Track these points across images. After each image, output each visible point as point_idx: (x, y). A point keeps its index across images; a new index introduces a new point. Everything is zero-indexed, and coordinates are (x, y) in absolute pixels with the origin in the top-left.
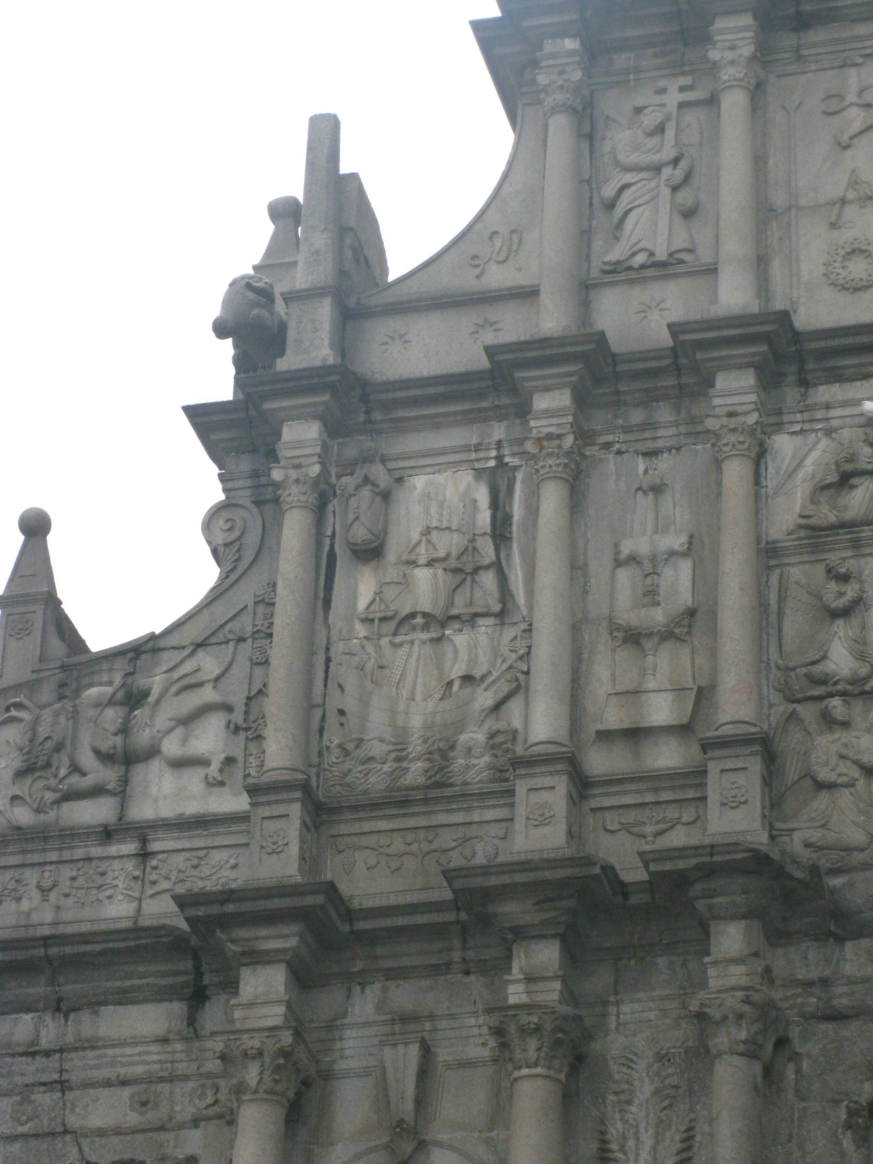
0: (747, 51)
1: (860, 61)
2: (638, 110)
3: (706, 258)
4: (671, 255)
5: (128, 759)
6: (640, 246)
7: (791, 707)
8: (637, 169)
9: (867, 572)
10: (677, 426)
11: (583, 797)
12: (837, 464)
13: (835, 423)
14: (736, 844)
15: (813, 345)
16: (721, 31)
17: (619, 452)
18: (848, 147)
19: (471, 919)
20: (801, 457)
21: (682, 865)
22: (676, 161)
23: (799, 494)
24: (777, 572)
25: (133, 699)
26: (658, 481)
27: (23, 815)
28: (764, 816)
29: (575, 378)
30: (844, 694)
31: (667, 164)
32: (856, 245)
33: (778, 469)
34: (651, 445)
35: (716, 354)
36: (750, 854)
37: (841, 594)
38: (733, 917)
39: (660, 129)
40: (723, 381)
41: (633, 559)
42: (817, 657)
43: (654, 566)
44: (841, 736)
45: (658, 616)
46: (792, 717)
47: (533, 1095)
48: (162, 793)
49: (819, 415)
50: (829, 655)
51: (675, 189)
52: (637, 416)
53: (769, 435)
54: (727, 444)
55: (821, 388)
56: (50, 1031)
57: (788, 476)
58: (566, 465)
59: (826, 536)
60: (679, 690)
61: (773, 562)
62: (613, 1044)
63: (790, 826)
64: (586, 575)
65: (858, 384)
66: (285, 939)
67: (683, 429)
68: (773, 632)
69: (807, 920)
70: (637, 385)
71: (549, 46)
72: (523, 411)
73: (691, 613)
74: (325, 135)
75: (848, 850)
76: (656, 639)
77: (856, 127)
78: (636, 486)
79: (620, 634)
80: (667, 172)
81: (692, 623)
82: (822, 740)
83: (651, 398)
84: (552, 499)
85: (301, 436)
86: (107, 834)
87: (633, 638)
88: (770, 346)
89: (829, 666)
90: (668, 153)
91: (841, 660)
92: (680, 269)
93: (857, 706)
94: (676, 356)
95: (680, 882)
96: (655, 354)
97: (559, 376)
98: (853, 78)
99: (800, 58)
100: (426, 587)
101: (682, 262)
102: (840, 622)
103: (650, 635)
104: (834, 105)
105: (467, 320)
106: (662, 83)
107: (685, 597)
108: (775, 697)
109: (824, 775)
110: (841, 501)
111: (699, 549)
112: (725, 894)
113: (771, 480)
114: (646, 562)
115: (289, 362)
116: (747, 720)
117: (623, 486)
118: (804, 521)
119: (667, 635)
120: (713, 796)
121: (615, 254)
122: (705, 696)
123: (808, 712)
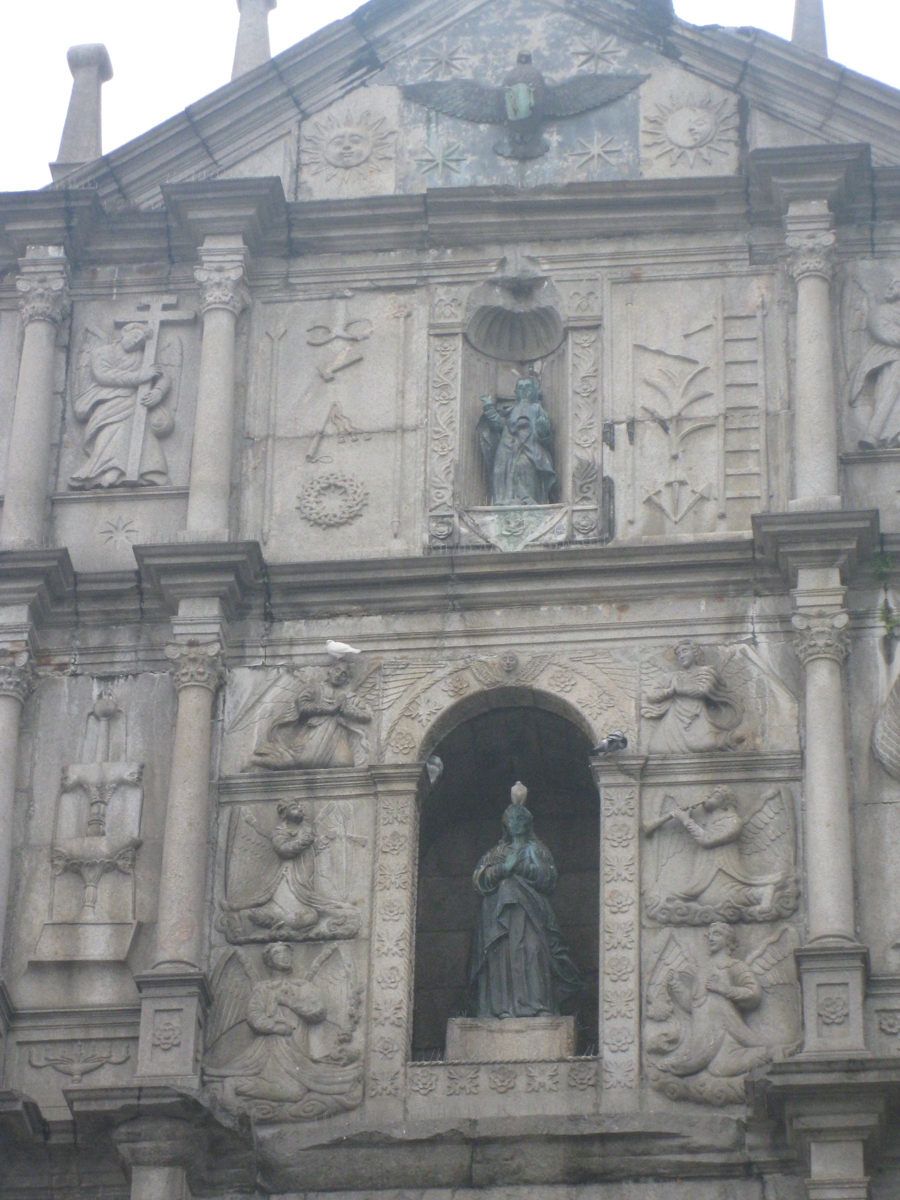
0: (235, 274)
1: (349, 294)
2: (119, 326)
3: (178, 481)
4: (142, 476)
6: (110, 464)
7: (232, 949)
8: (114, 385)
9: (320, 815)
10: (136, 652)
11: (9, 1030)
12: (297, 702)
13: (298, 660)
14: (166, 1088)
15: (281, 579)
16: (210, 252)
17: (74, 675)
18: (331, 379)
20: (260, 693)
21: (108, 1106)
22: (154, 381)
23: (256, 731)
24: (227, 811)
26: (111, 707)
28: (196, 1060)
29: (34, 595)
30: (287, 939)
31: (144, 383)
32: (332, 481)
33: (238, 702)
34: (108, 669)
35: (180, 581)
36: (179, 1099)
37: (292, 836)
38: (157, 1164)
39: (140, 347)
40: (185, 609)
41: (80, 786)
42: (263, 899)
43: (102, 795)
44: (281, 983)
45: (102, 846)
46: (233, 959)
49: (282, 651)
50: (275, 898)
51: (151, 409)
52: (95, 639)
53: (230, 668)
54: (186, 674)
55: (286, 623)
57: (247, 712)
58: (18, 684)
59: (280, 776)
60: (118, 924)
61: (224, 799)
63: (223, 1072)
64: (30, 801)
65: (325, 622)
67: (141, 655)
68: (220, 871)
69: (233, 1171)
70: (97, 607)
71: (32, 253)
73: (137, 846)
75: (281, 1100)
76: (98, 870)
77: (341, 360)
78: (90, 710)
79: (60, 863)
80: (144, 390)
81: (137, 856)
82: (262, 986)
83: (111, 621)
87: (74, 868)
88: (237, 577)
89: (275, 910)
90: (147, 371)
91: (286, 905)
92: (149, 491)
93: (301, 951)
94: (140, 580)
95: (104, 1124)
96: (118, 576)
97: (16, 591)
99: (288, 286)
101: (153, 484)
102: (289, 865)
103: (92, 865)
104: (320, 336)
106: (145, 300)
107: (131, 829)
108: (216, 938)
109: (261, 1021)
110: (298, 741)
111: (150, 780)
112: (151, 1140)
113: (228, 714)
114: (94, 790)
116: (185, 959)
117: (75, 710)
118: (258, 759)
119: (110, 867)
120: (146, 1035)
121: (85, 470)
122: (144, 931)
123: (249, 956)
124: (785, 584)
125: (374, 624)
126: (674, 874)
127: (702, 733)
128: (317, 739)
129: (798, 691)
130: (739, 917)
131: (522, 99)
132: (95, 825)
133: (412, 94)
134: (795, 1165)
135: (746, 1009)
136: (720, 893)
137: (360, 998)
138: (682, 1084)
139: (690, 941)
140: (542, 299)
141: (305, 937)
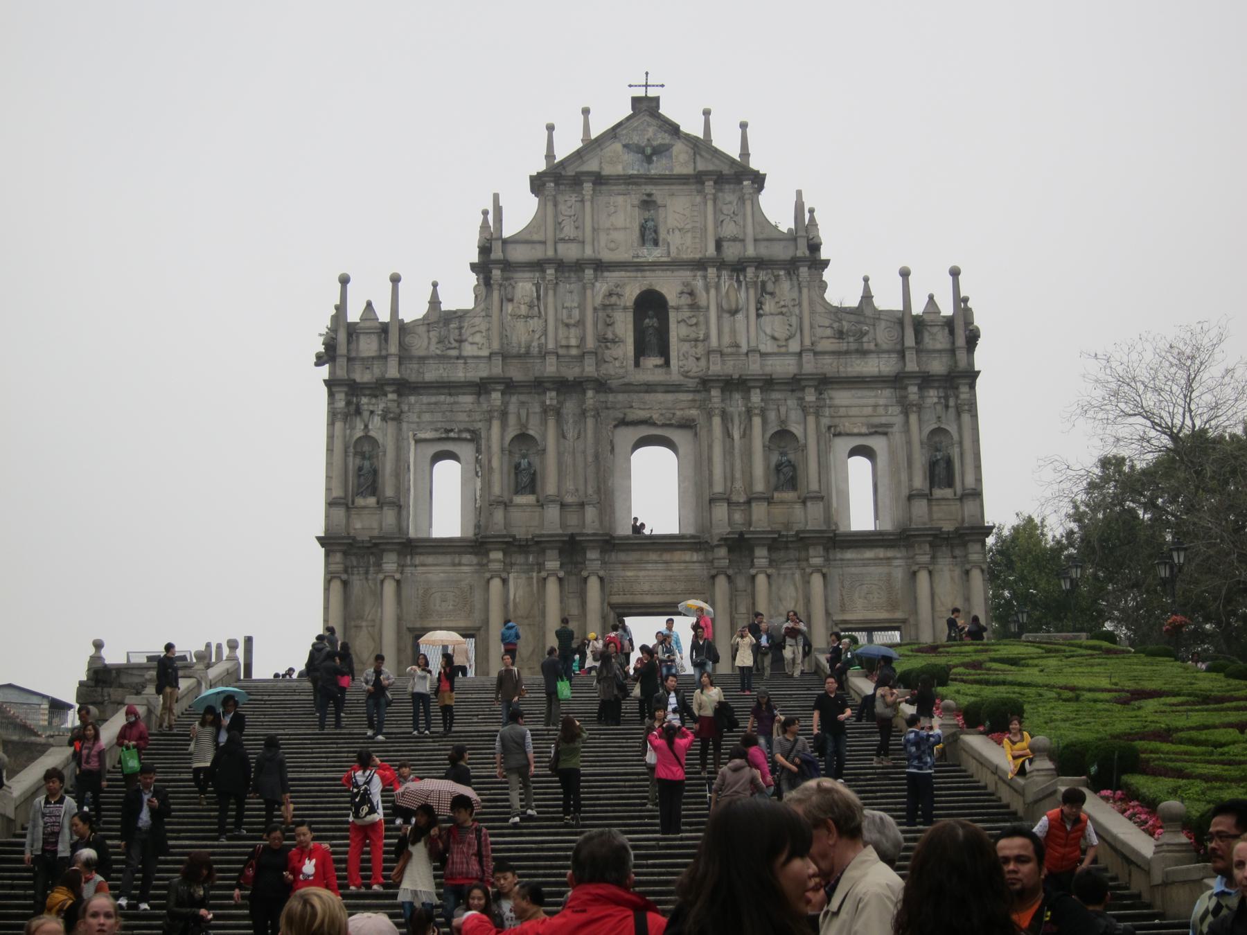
5: (460, 341)
19: (538, 385)
25: (460, 328)
27: (439, 352)
45: (572, 321)
47: (551, 423)
48: (468, 350)
56: (449, 399)
62: (564, 411)
66: (501, 387)
72: (543, 271)
74: (496, 197)
83: (570, 271)
84: (551, 293)
85: (496, 273)
86: (458, 358)
87: (567, 325)
91: (610, 336)
98: (612, 199)
100: (524, 310)
105: (529, 246)
107: (577, 318)
111: (582, 307)
115: (493, 256)
121: (562, 236)
122: (583, 339)
124: (706, 270)
125: (623, 274)
126: (684, 330)
127: (689, 301)
128: (614, 299)
129: (708, 292)
130: (696, 340)
131: (649, 151)
132: (570, 316)
133: (625, 146)
134: (708, 391)
135: (698, 359)
136: (693, 336)
137: (625, 354)
138: (686, 375)
139: (687, 345)
140: (654, 198)
141: (614, 342)
